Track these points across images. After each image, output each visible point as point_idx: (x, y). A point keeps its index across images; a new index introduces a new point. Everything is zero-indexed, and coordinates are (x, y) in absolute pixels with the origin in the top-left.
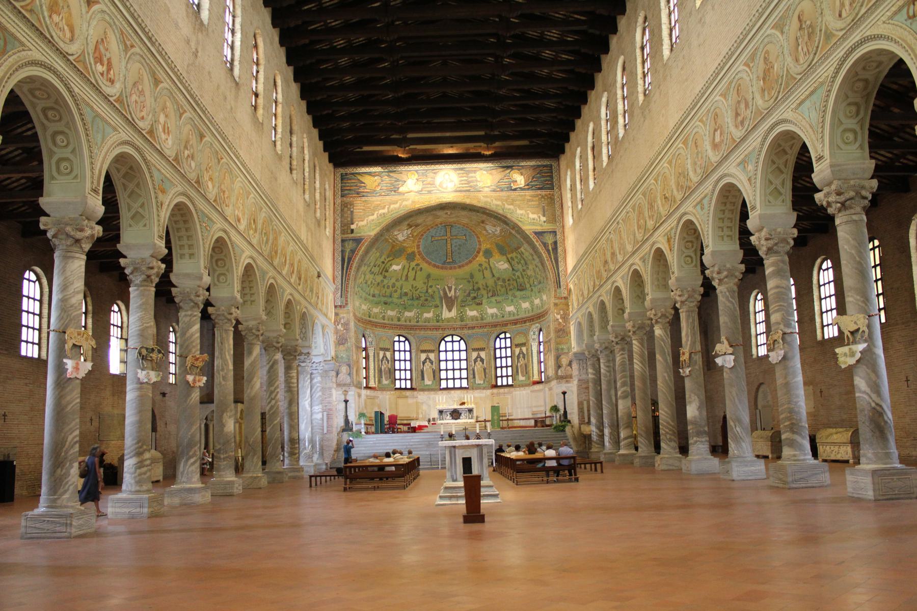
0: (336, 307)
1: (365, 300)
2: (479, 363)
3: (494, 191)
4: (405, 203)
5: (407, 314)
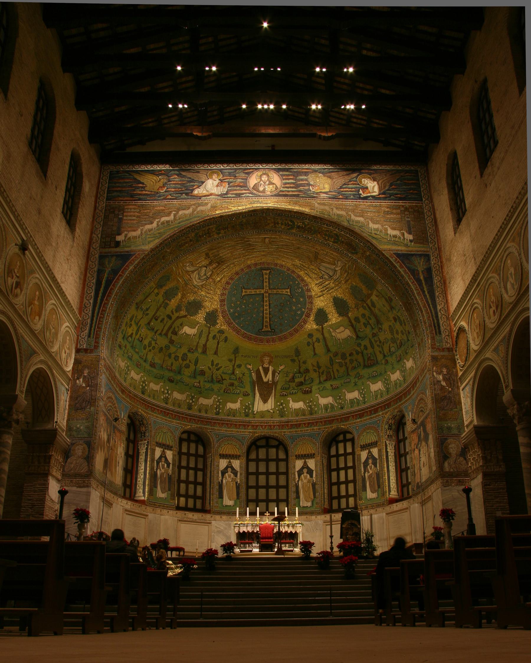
0: (78, 351)
1: (138, 365)
2: (305, 476)
3: (335, 198)
5: (203, 401)
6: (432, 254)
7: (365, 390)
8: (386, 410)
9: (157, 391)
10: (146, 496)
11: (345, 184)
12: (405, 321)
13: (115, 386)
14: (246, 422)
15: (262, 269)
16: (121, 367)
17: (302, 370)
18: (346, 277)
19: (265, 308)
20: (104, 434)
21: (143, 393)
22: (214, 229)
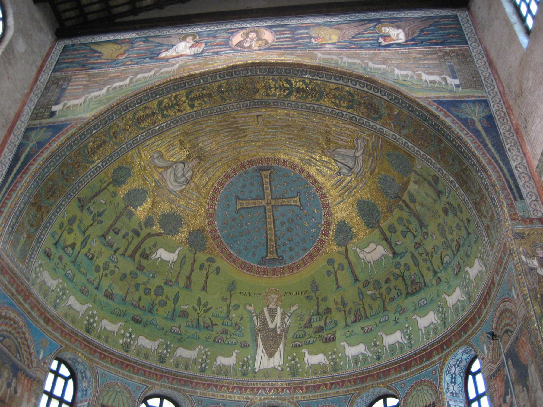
1: (83, 291)
5: (182, 352)
6: (492, 99)
7: (411, 328)
8: (445, 352)
9: (114, 332)
11: (358, 34)
12: (461, 204)
13: (27, 306)
15: (260, 170)
16: (49, 284)
17: (321, 310)
18: (371, 166)
19: (269, 226)
21: (88, 331)
22: (184, 99)
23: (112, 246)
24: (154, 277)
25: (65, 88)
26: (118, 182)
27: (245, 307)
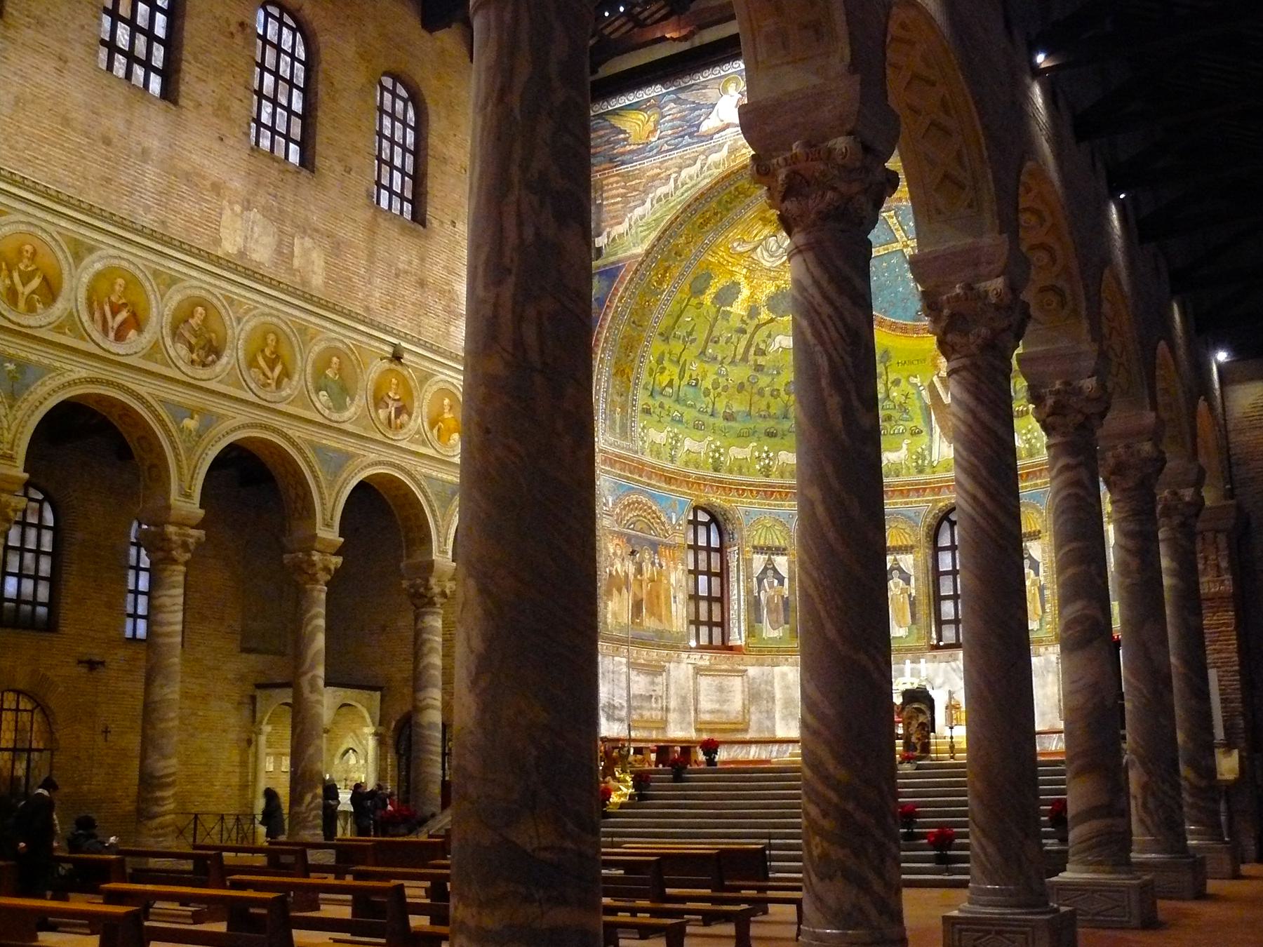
1: (697, 427)
4: (714, 158)
10: (743, 639)
14: (919, 484)
20: (623, 565)
21: (716, 470)
23: (715, 359)
24: (778, 373)
25: (601, 204)
26: (698, 291)
27: (908, 380)
